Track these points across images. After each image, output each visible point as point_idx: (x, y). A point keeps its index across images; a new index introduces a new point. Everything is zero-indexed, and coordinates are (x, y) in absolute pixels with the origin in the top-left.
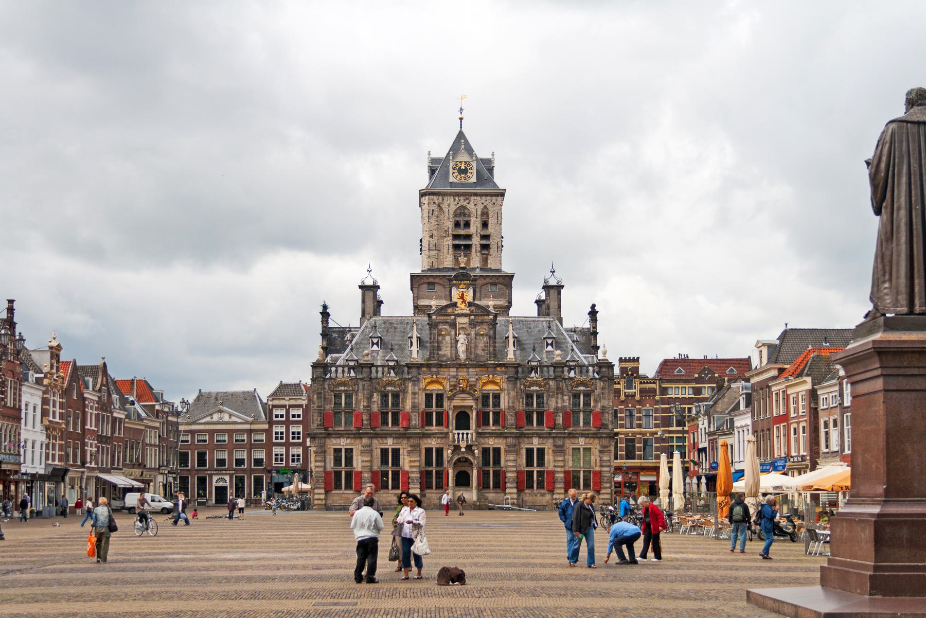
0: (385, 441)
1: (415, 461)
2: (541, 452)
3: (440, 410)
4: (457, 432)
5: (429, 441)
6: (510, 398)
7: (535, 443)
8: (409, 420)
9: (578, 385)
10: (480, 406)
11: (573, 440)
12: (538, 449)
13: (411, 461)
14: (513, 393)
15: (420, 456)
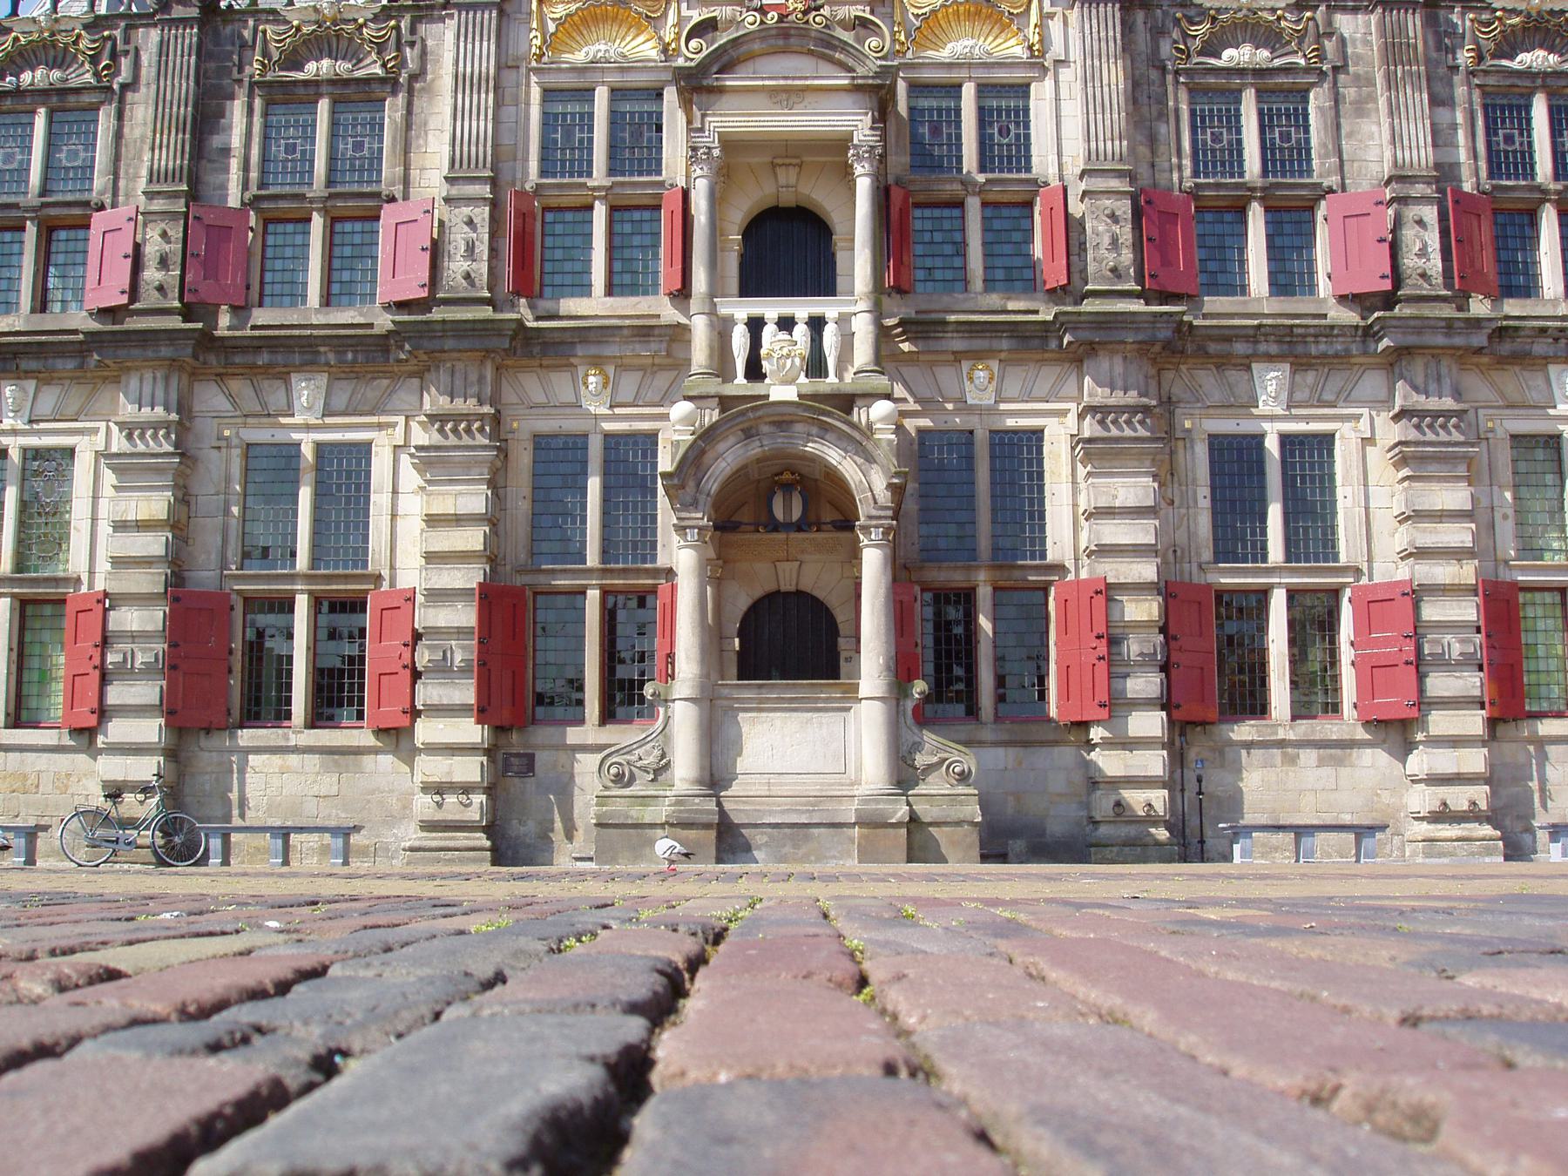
0: (276, 398)
1: (458, 520)
2: (1309, 455)
3: (637, 184)
4: (740, 310)
5: (561, 386)
6: (1092, 105)
7: (1272, 406)
8: (436, 251)
9: (1510, 45)
10: (900, 161)
11: (1512, 381)
12: (1286, 440)
13: (433, 521)
14: (1115, 76)
15: (496, 485)
